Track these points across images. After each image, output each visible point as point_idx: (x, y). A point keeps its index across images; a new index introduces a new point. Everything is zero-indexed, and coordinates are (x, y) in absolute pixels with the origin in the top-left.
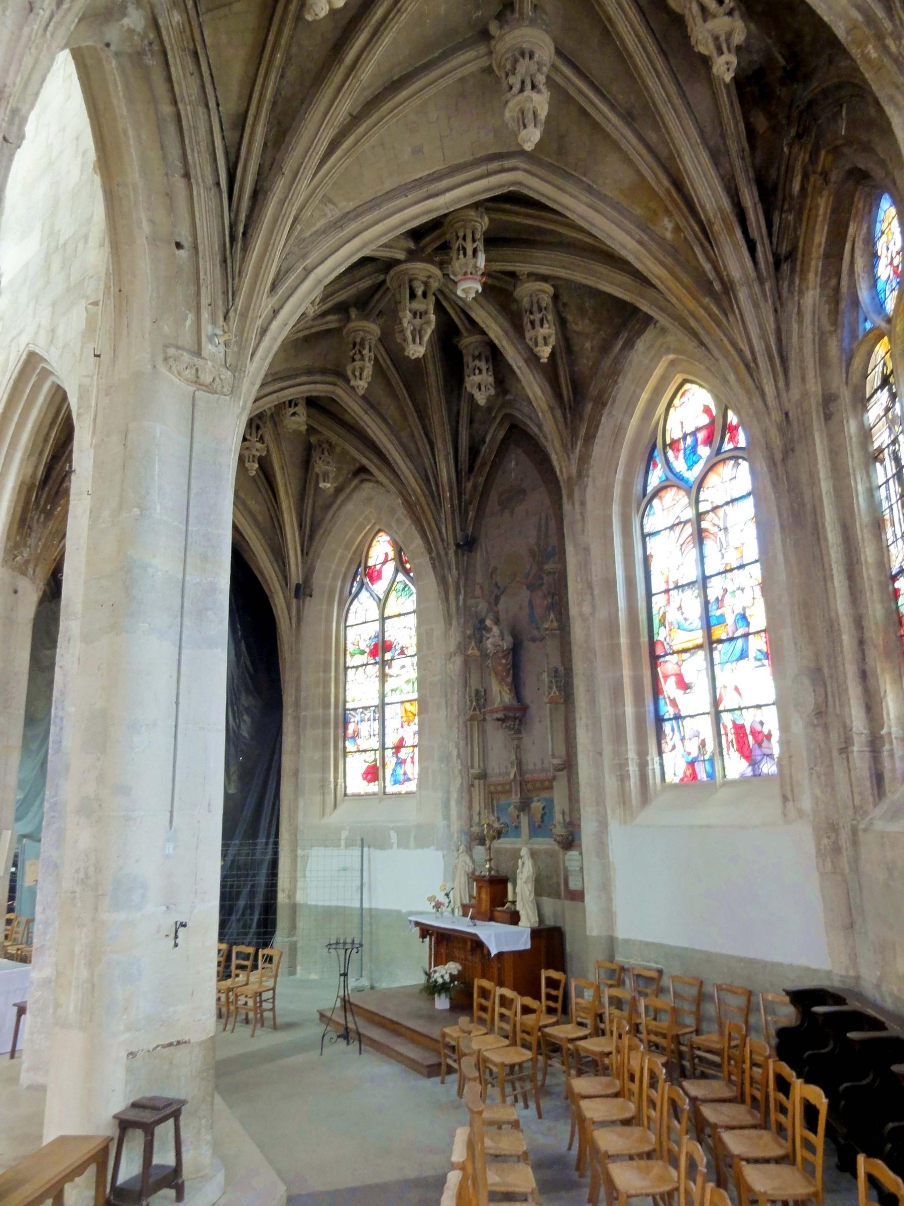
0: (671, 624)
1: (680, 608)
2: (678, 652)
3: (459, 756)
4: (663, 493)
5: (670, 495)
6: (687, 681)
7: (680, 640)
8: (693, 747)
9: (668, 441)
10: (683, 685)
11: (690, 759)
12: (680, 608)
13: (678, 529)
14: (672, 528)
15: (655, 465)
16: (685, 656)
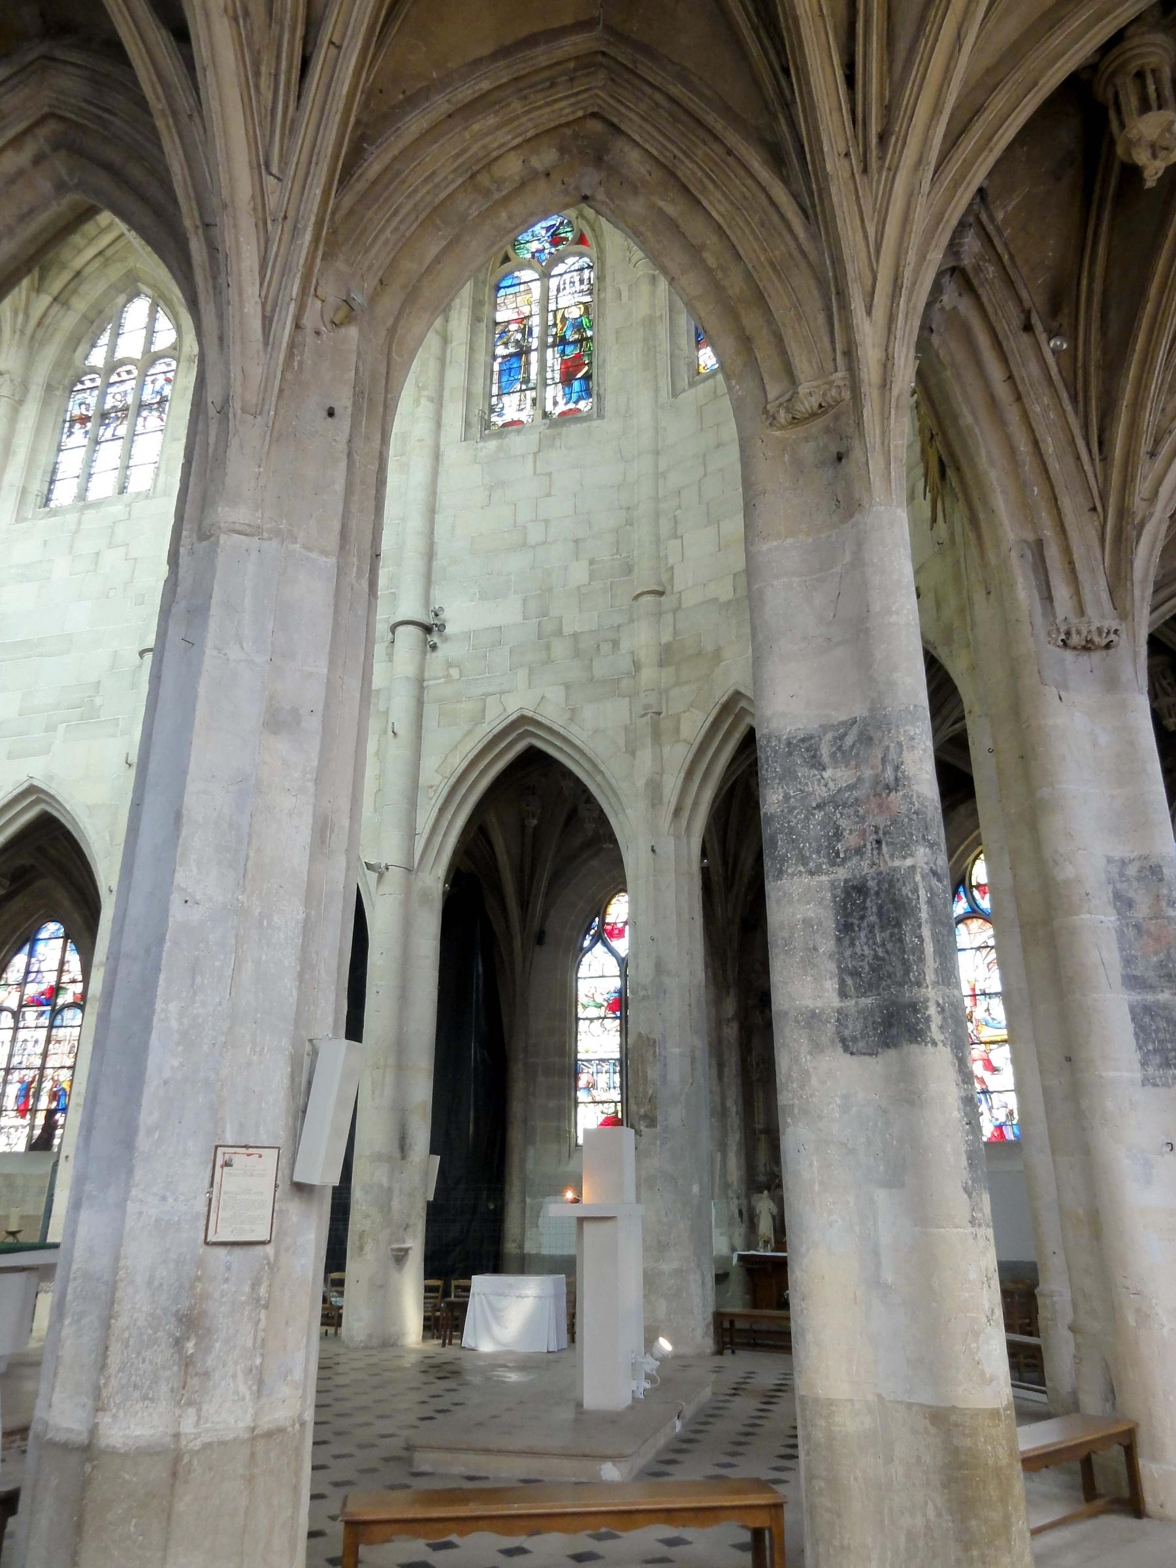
0: (978, 1021)
1: (988, 1010)
2: (985, 1043)
3: (737, 1113)
4: (969, 922)
5: (975, 924)
6: (995, 1064)
7: (986, 1034)
8: (1001, 1116)
9: (974, 883)
10: (990, 1066)
11: (998, 1123)
12: (988, 1010)
13: (985, 952)
14: (979, 948)
15: (960, 898)
16: (992, 1046)
